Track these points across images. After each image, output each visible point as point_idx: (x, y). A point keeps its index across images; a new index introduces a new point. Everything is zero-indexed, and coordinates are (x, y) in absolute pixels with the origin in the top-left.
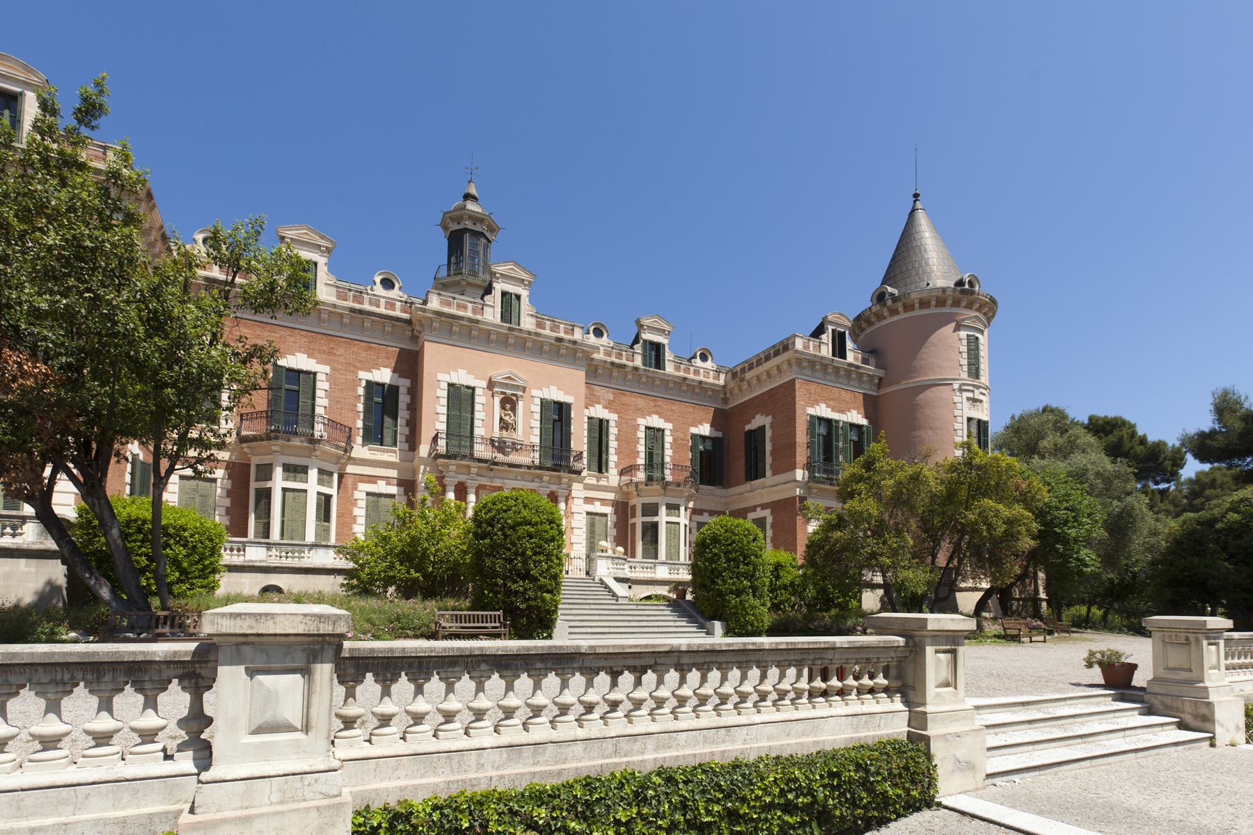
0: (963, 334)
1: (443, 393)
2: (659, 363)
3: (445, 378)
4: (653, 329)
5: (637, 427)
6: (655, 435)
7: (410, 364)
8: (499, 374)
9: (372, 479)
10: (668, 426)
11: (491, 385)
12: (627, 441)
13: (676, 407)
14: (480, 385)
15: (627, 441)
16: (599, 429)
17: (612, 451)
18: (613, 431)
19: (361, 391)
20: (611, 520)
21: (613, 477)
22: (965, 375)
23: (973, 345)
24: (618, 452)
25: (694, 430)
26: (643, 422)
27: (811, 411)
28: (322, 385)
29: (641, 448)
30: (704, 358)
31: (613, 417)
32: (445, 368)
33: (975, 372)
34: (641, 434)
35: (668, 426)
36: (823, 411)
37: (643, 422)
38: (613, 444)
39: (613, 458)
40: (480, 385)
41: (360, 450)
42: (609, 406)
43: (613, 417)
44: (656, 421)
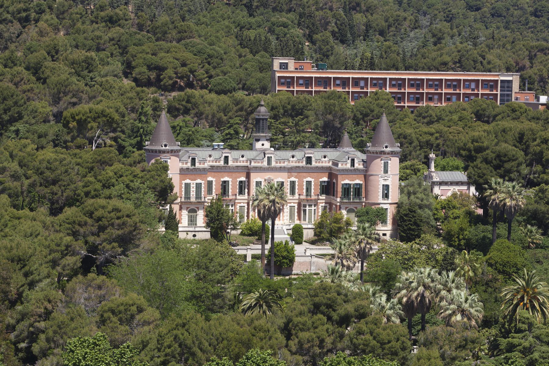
0: (383, 162)
1: (255, 184)
2: (311, 163)
3: (255, 180)
4: (308, 153)
5: (303, 182)
6: (309, 183)
7: (248, 176)
8: (266, 178)
9: (240, 203)
10: (312, 180)
11: (265, 180)
12: (301, 186)
13: (315, 174)
14: (263, 180)
15: (301, 186)
16: (293, 184)
17: (296, 189)
18: (297, 183)
19: (238, 183)
20: (296, 207)
21: (297, 196)
22: (383, 173)
23: (386, 165)
24: (298, 189)
25: (321, 180)
26: (305, 180)
27: (343, 182)
28: (230, 183)
29: (305, 187)
30: (325, 157)
31: (296, 180)
32: (255, 178)
33: (386, 171)
34: (305, 183)
35: (312, 180)
36: (347, 181)
37: (305, 180)
38: (297, 187)
39: (297, 191)
40: (263, 180)
41: (238, 197)
42: (296, 177)
43: (296, 180)
44: (309, 179)
